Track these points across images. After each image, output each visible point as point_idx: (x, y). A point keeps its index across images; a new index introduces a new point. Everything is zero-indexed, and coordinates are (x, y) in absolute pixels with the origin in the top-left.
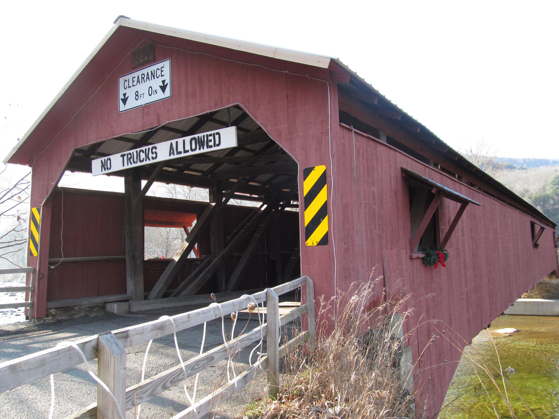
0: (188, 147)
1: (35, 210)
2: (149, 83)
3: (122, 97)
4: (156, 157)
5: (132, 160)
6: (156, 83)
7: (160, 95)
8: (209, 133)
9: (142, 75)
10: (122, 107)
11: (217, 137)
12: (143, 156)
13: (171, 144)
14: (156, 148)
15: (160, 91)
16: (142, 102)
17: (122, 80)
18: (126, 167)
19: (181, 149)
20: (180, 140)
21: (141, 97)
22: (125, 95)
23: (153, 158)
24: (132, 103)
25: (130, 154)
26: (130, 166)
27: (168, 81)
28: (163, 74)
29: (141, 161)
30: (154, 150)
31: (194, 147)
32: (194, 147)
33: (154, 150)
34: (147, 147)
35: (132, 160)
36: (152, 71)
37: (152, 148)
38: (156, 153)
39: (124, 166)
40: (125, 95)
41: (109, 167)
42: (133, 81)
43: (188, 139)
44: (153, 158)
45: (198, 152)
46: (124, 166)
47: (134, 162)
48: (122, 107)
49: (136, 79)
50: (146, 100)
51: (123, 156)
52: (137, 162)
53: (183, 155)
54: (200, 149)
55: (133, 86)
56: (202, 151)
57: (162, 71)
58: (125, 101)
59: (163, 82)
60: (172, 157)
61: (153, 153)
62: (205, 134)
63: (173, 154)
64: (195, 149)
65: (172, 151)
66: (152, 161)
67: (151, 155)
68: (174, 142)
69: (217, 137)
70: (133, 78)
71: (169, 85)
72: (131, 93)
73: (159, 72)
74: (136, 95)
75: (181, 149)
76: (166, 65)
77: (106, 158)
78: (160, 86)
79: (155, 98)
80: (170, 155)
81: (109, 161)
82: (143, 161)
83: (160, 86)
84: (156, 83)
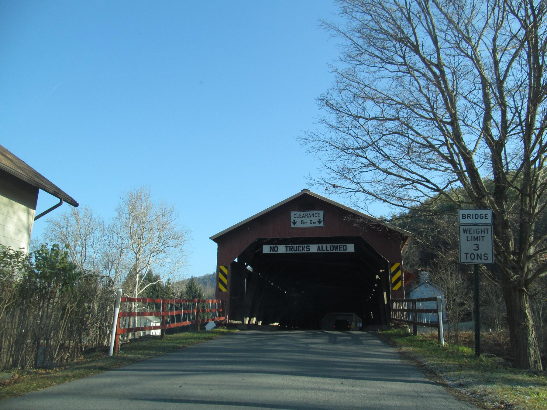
0: (328, 248)
1: (222, 268)
2: (310, 218)
3: (292, 220)
4: (309, 250)
5: (293, 249)
6: (315, 219)
7: (317, 225)
8: (340, 245)
10: (292, 225)
12: (300, 248)
13: (319, 246)
14: (309, 246)
15: (317, 223)
16: (304, 225)
17: (292, 214)
18: (288, 252)
19: (324, 248)
20: (324, 246)
22: (294, 220)
23: (307, 250)
24: (299, 225)
25: (292, 246)
26: (291, 252)
27: (322, 219)
29: (299, 251)
30: (308, 247)
31: (332, 249)
32: (332, 249)
33: (308, 247)
34: (304, 245)
35: (293, 249)
37: (307, 246)
38: (309, 249)
39: (287, 251)
40: (294, 220)
41: (276, 250)
43: (328, 246)
47: (294, 251)
48: (292, 225)
49: (302, 215)
50: (309, 225)
51: (287, 247)
52: (296, 251)
53: (325, 252)
56: (336, 251)
58: (294, 223)
59: (320, 219)
60: (319, 252)
61: (307, 248)
62: (339, 245)
64: (333, 250)
66: (306, 252)
67: (305, 249)
68: (320, 245)
71: (323, 222)
72: (299, 221)
73: (317, 215)
75: (324, 248)
76: (321, 213)
77: (274, 246)
79: (313, 225)
81: (276, 248)
82: (301, 250)
84: (315, 219)
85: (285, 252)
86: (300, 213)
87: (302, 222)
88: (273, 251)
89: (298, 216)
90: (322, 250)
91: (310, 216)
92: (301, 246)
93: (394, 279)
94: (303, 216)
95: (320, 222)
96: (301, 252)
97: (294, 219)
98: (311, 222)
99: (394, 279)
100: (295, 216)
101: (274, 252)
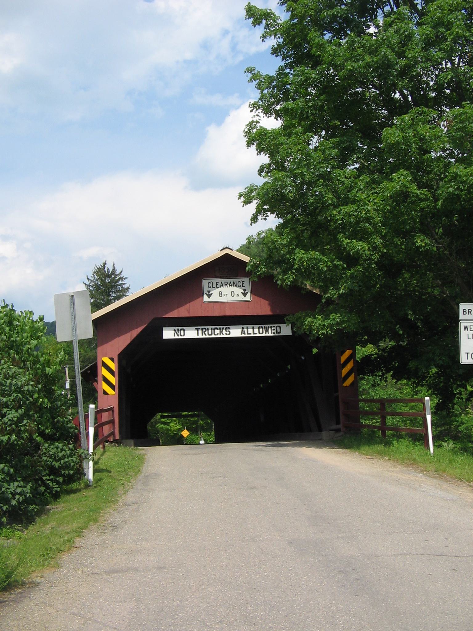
4: (229, 334)
9: (225, 282)
11: (278, 329)
17: (205, 282)
21: (224, 296)
23: (226, 334)
28: (243, 285)
32: (261, 331)
36: (234, 282)
39: (198, 335)
42: (217, 285)
44: (226, 334)
45: (264, 335)
46: (198, 335)
49: (219, 284)
50: (229, 298)
52: (211, 335)
53: (252, 335)
54: (266, 333)
55: (217, 287)
56: (267, 335)
57: (243, 284)
58: (209, 296)
60: (243, 335)
63: (244, 333)
64: (262, 333)
65: (243, 332)
69: (278, 329)
70: (217, 282)
73: (240, 284)
74: (220, 294)
78: (242, 293)
79: (235, 299)
80: (242, 334)
82: (218, 334)
83: (242, 293)
85: (196, 337)
86: (217, 280)
87: (220, 294)
88: (178, 335)
89: (215, 285)
90: (248, 334)
91: (230, 285)
92: (217, 329)
93: (345, 371)
94: (222, 286)
95: (245, 294)
96: (219, 336)
97: (209, 289)
98: (233, 294)
99: (345, 371)
100: (210, 285)
101: (180, 337)
